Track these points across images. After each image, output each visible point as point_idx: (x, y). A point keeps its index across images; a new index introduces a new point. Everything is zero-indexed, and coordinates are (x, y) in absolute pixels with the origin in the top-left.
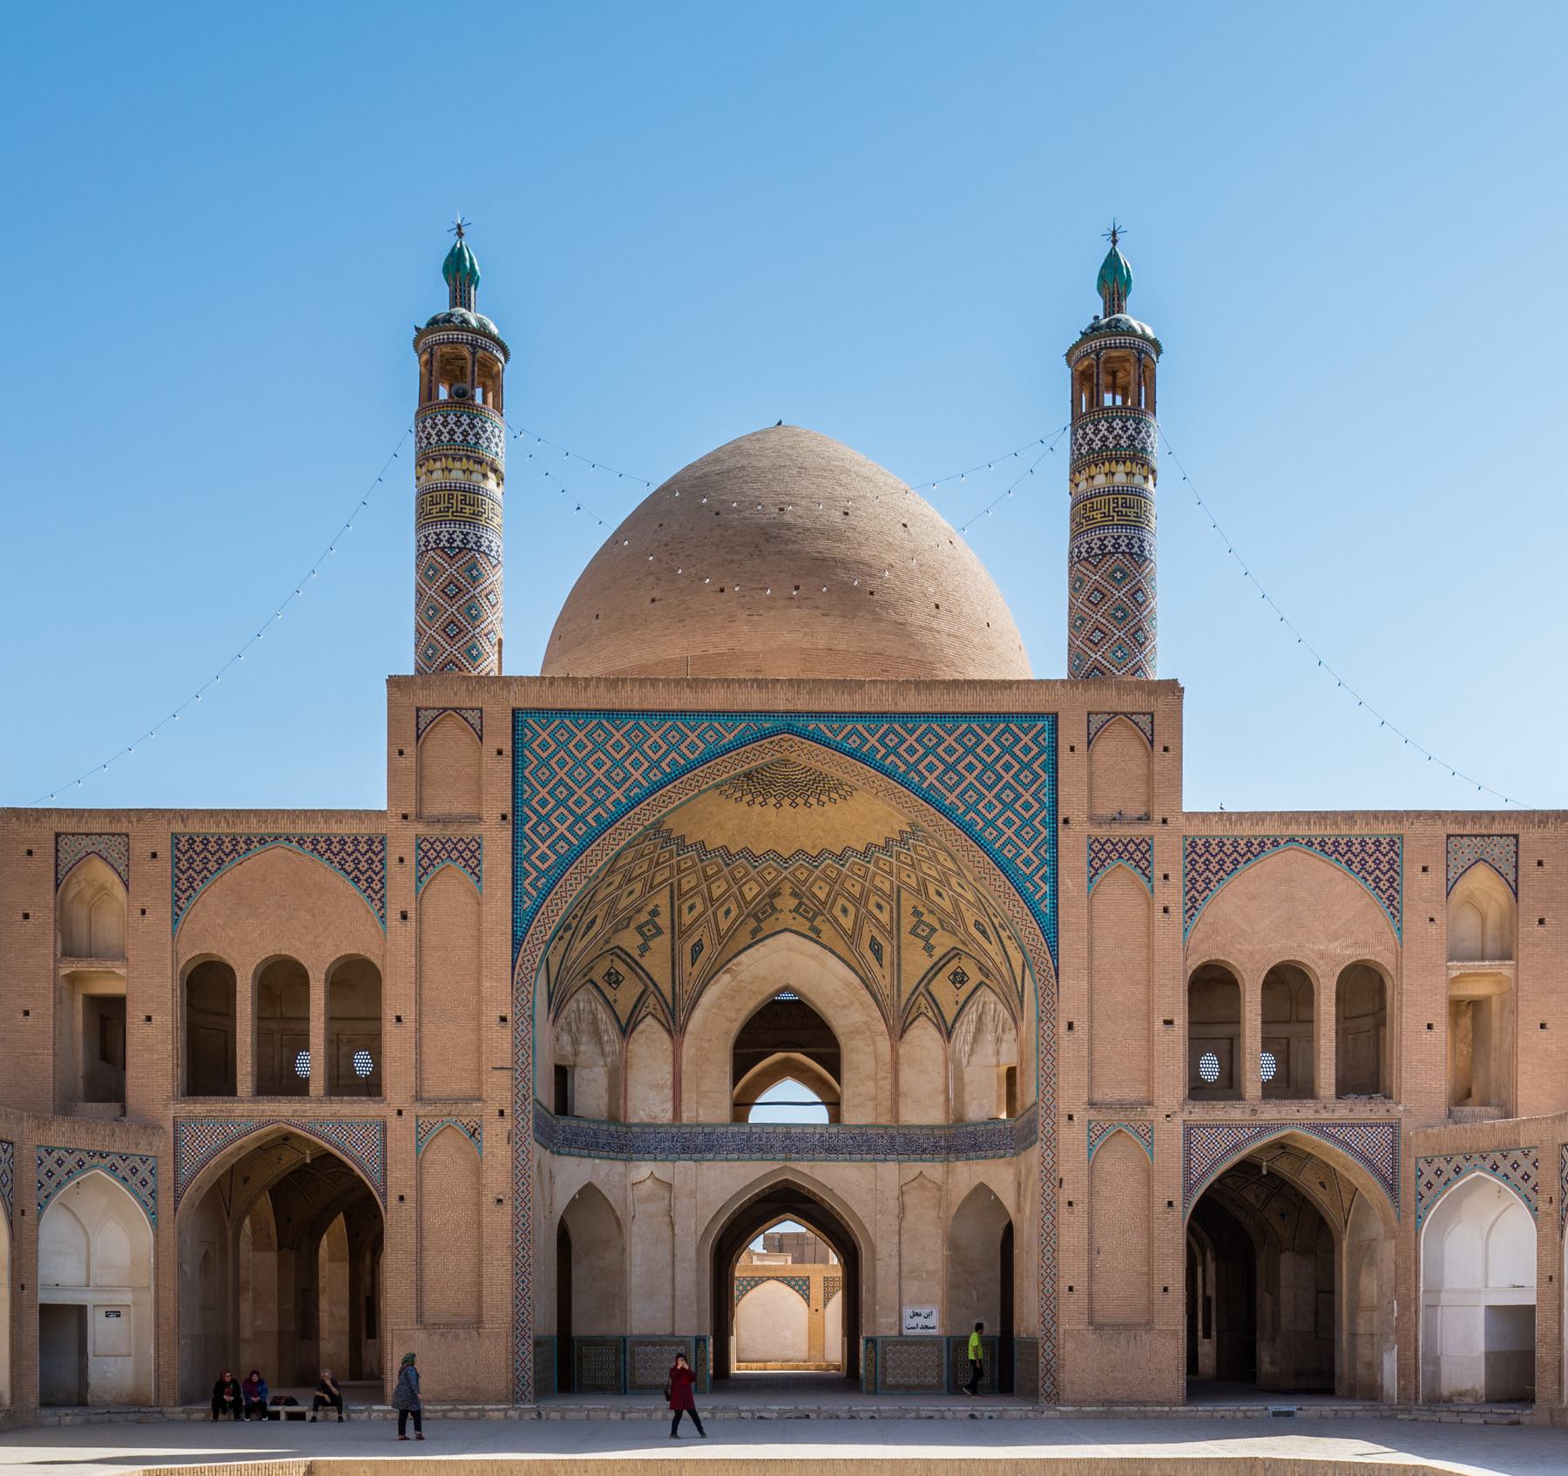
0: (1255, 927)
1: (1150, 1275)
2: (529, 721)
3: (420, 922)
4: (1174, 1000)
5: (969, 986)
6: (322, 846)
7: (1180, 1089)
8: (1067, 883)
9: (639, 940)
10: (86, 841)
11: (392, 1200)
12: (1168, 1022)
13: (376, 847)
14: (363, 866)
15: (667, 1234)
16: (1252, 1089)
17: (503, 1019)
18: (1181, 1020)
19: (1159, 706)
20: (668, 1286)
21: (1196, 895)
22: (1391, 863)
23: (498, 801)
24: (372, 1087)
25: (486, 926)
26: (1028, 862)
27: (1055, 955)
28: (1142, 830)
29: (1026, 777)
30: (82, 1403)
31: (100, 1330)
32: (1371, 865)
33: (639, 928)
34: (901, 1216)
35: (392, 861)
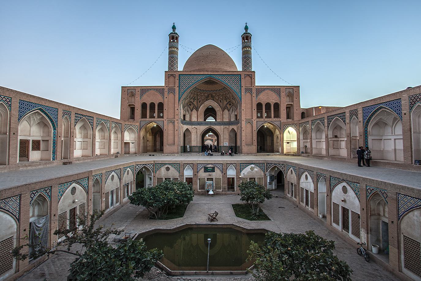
0: (264, 98)
1: (253, 139)
2: (181, 75)
3: (168, 98)
4: (255, 107)
5: (231, 105)
6: (157, 90)
7: (256, 117)
8: (242, 93)
9: (193, 100)
10: (131, 90)
11: (164, 130)
12: (254, 109)
13: (163, 90)
14: (162, 92)
15: (196, 134)
16: (264, 117)
17: (177, 109)
18: (256, 109)
19: (252, 74)
20: (196, 140)
21: (257, 95)
22: (279, 91)
23: (177, 84)
24: (162, 117)
25: (175, 98)
26: (238, 91)
27: (241, 102)
28: (251, 88)
29: (237, 82)
30: (129, 154)
31: (131, 145)
32: (277, 92)
33: (193, 99)
34: (224, 132)
35: (165, 92)
